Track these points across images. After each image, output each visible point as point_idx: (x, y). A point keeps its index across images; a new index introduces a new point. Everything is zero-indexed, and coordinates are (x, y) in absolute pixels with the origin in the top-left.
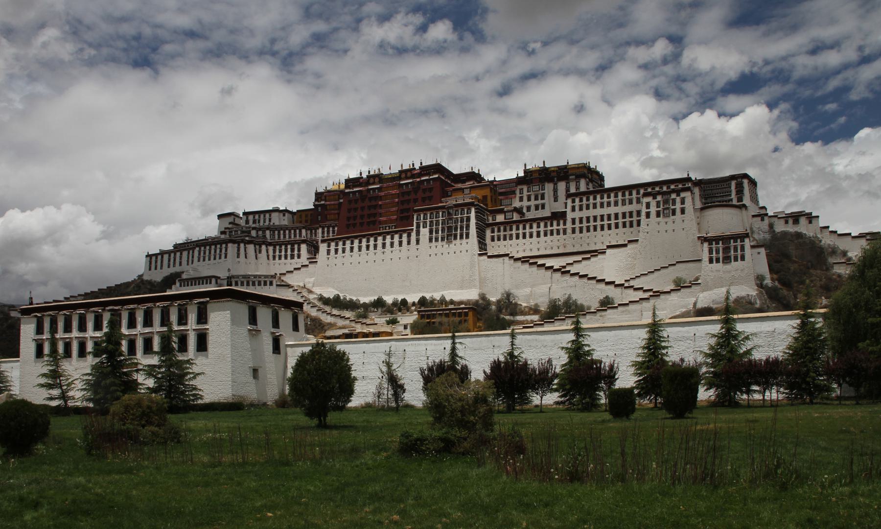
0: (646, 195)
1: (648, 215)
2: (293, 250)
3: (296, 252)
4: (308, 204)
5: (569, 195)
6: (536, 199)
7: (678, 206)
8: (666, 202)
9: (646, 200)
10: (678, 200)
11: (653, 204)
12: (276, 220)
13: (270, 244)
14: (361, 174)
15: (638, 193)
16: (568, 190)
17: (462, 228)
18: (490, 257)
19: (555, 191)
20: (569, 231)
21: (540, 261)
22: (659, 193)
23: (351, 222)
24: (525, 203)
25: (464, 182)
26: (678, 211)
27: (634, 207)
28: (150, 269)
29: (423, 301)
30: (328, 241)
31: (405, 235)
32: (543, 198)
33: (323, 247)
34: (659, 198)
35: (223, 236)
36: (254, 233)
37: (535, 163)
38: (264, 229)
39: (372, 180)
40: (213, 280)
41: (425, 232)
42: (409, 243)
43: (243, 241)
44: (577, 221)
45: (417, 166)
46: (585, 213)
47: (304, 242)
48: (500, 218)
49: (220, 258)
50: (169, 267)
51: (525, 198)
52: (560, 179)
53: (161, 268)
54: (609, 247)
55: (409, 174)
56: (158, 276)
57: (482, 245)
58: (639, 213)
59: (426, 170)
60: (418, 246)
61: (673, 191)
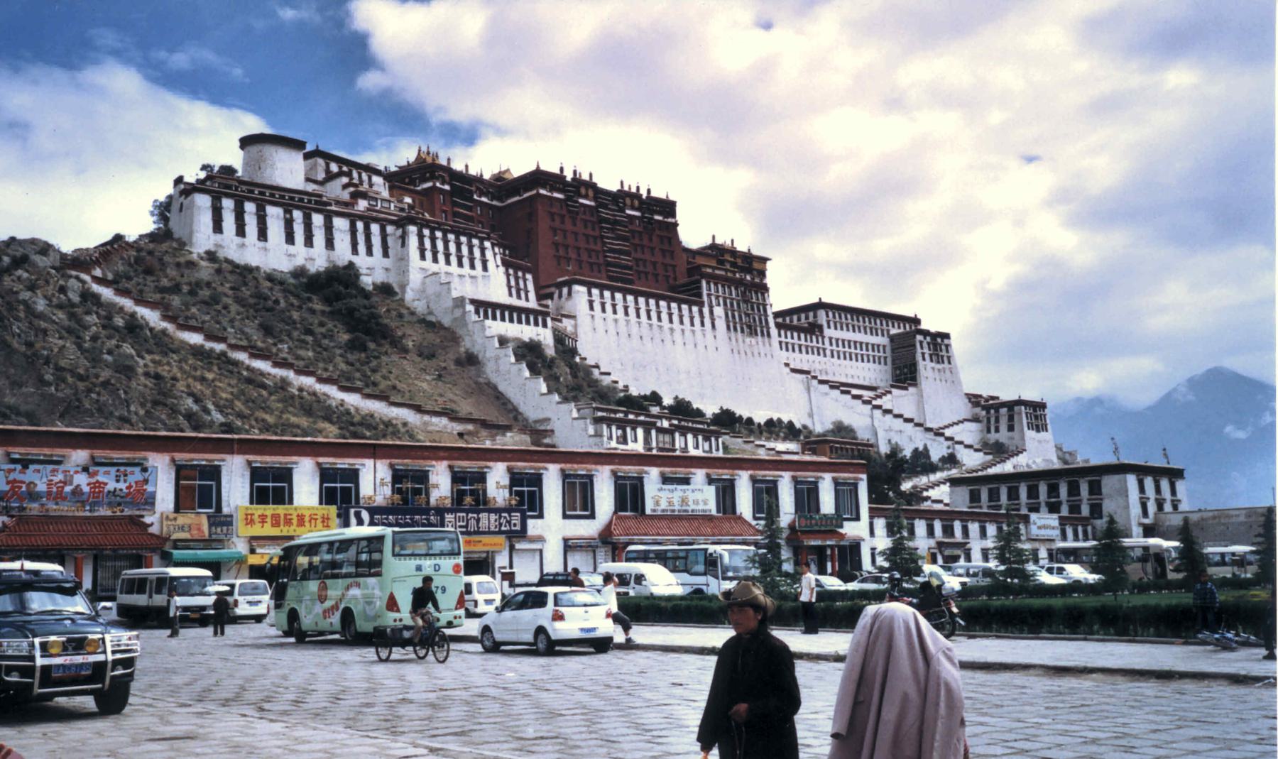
2: (517, 279)
8: (935, 345)
9: (919, 337)
11: (925, 345)
14: (562, 169)
18: (794, 371)
20: (828, 353)
21: (855, 392)
28: (218, 227)
29: (770, 423)
30: (590, 285)
31: (695, 309)
39: (583, 191)
40: (549, 320)
41: (719, 311)
42: (703, 324)
49: (473, 267)
50: (290, 239)
53: (263, 234)
55: (636, 203)
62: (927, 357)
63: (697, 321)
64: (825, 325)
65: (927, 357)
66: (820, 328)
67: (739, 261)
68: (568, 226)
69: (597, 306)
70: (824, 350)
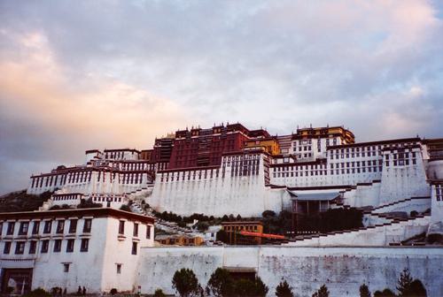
0: (386, 149)
1: (388, 165)
2: (137, 176)
3: (139, 178)
4: (150, 146)
5: (328, 148)
6: (305, 149)
7: (410, 158)
8: (401, 156)
9: (386, 153)
10: (410, 154)
12: (129, 156)
13: (122, 173)
15: (380, 148)
16: (328, 143)
17: (254, 167)
19: (319, 145)
20: (329, 172)
22: (395, 148)
23: (179, 159)
24: (297, 151)
25: (256, 136)
26: (411, 162)
27: (377, 157)
29: (226, 219)
32: (310, 149)
33: (159, 176)
34: (396, 152)
35: (89, 166)
36: (111, 165)
37: (304, 125)
38: (117, 162)
40: (79, 196)
41: (229, 169)
42: (217, 176)
43: (103, 170)
44: (335, 166)
45: (225, 126)
46: (340, 160)
47: (145, 172)
48: (280, 161)
51: (298, 149)
52: (322, 137)
54: (358, 184)
56: (38, 191)
57: (267, 179)
58: (381, 162)
59: (231, 127)
60: (225, 179)
61: (407, 147)
62: (391, 164)
63: (215, 175)
64: (329, 157)
65: (391, 164)
66: (325, 161)
67: (318, 133)
68: (185, 148)
69: (165, 180)
70: (326, 172)
